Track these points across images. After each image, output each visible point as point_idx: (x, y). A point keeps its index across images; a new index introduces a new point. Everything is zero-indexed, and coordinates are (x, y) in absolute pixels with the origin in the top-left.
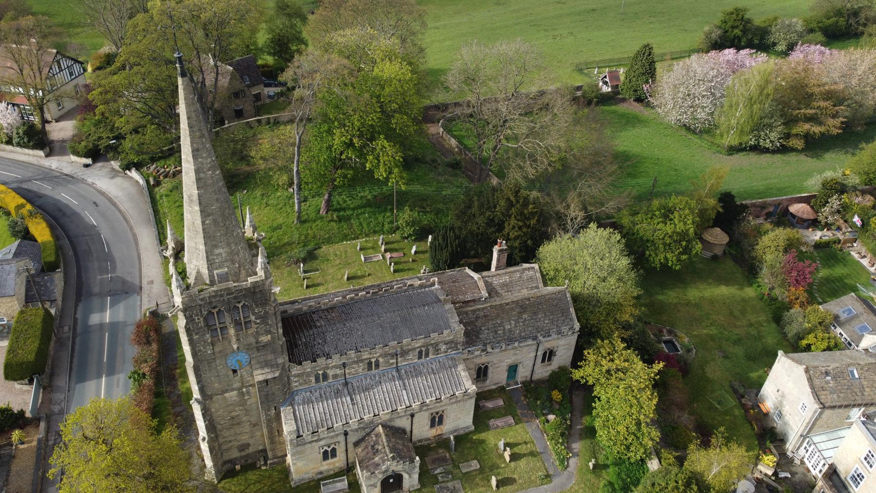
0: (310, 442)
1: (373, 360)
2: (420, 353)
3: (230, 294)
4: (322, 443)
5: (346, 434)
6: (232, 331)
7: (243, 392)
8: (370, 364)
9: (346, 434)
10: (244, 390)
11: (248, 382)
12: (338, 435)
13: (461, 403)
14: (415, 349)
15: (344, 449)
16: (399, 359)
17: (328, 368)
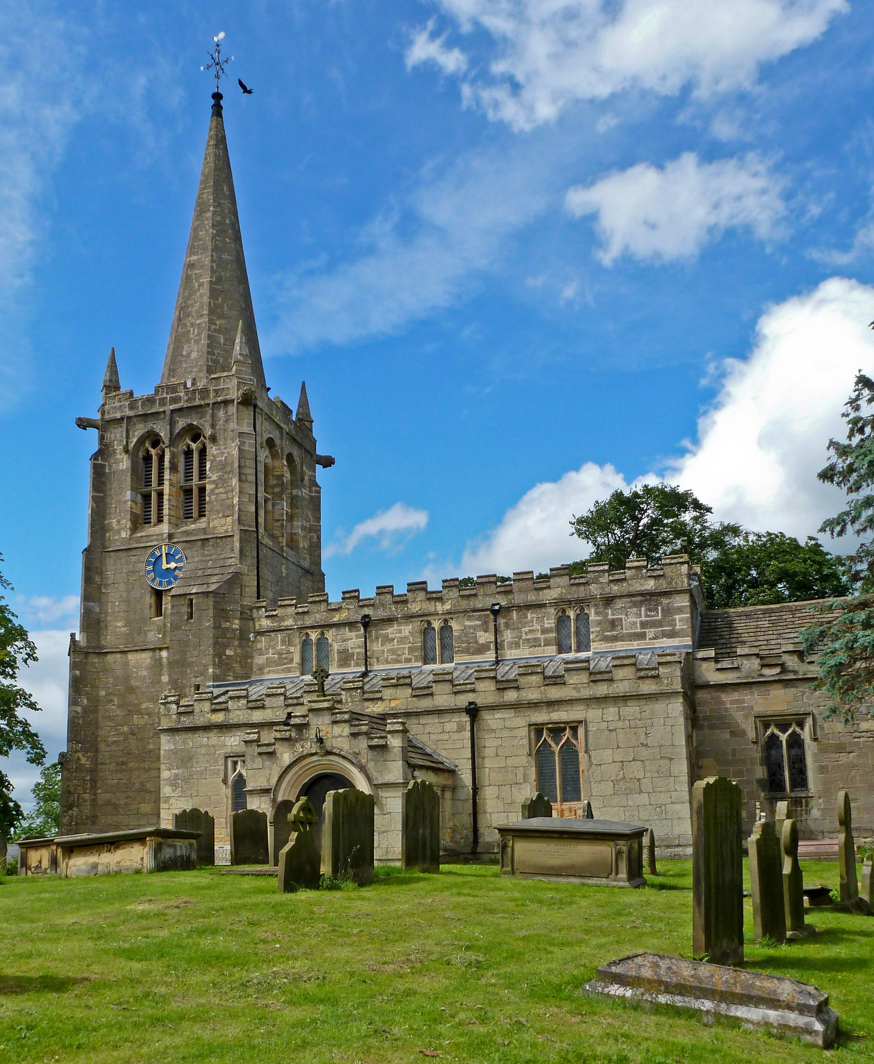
0: (207, 728)
1: (436, 624)
2: (562, 620)
7: (161, 658)
8: (427, 631)
13: (632, 710)
14: (542, 606)
16: (508, 636)
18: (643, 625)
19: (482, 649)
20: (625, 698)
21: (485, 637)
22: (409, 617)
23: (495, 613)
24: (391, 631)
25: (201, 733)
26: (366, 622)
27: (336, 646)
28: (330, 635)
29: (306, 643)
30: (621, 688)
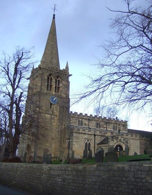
0: (82, 133)
2: (114, 126)
3: (57, 70)
4: (86, 136)
5: (95, 135)
6: (54, 86)
9: (95, 135)
10: (53, 116)
11: (55, 113)
12: (92, 135)
14: (112, 123)
15: (94, 146)
16: (108, 127)
17: (83, 119)
18: (123, 129)
19: (105, 128)
20: (134, 139)
21: (105, 126)
22: (95, 120)
23: (106, 123)
24: (92, 122)
25: (81, 134)
26: (89, 120)
27: (84, 122)
28: (83, 120)
29: (79, 121)
30: (134, 138)
